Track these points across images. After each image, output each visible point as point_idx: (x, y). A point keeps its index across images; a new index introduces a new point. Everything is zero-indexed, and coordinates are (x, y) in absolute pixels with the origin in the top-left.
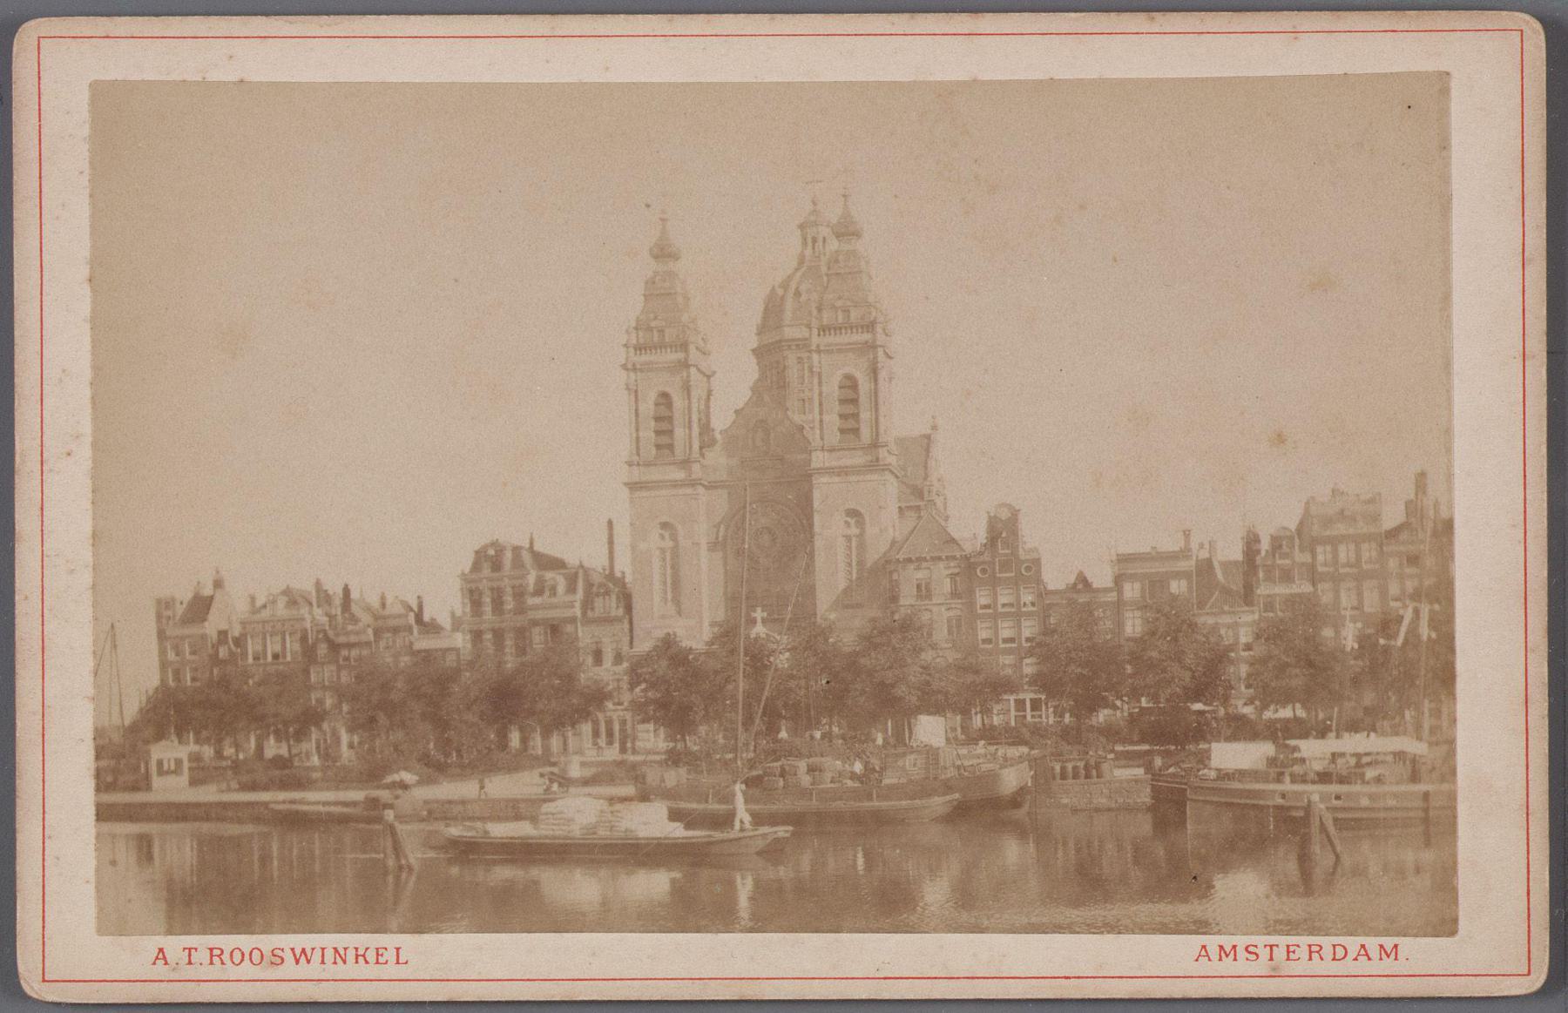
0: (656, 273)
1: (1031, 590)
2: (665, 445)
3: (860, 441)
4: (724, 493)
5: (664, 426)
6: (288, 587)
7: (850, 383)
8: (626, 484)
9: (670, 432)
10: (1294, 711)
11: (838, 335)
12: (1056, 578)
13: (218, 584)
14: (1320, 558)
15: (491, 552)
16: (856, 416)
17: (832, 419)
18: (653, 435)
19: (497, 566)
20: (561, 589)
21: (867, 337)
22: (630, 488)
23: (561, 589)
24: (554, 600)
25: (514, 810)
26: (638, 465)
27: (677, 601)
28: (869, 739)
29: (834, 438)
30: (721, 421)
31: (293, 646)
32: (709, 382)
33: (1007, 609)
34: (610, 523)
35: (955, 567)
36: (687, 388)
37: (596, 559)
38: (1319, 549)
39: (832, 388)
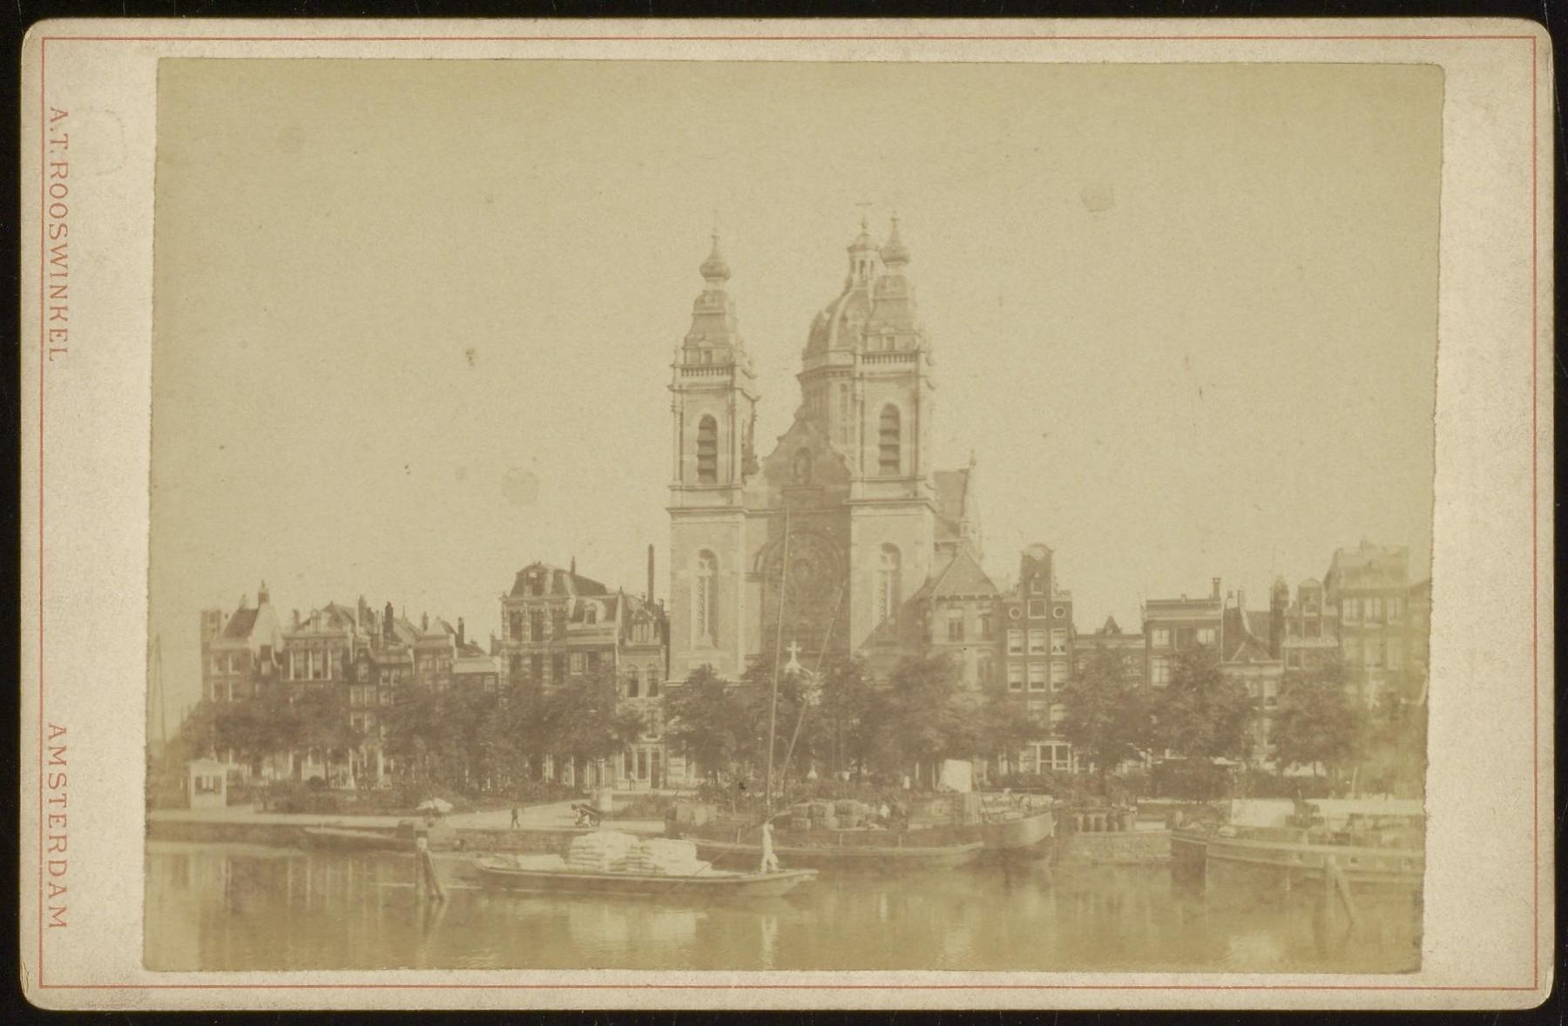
0: (705, 293)
1: (1062, 634)
2: (708, 472)
3: (898, 472)
4: (764, 521)
5: (708, 451)
6: (332, 603)
7: (891, 413)
8: (668, 509)
9: (714, 457)
10: (1315, 769)
11: (887, 363)
12: (1087, 622)
13: (263, 598)
14: (1346, 611)
15: (533, 575)
16: (896, 448)
17: (873, 449)
18: (697, 460)
19: (538, 589)
20: (601, 613)
21: (909, 366)
22: (672, 513)
23: (601, 613)
24: (592, 626)
25: (559, 842)
26: (681, 490)
27: (713, 632)
28: (897, 782)
29: (873, 468)
30: (764, 447)
31: (334, 663)
32: (753, 406)
33: (1038, 653)
34: (651, 549)
35: (987, 607)
36: (731, 411)
37: (637, 588)
38: (1346, 603)
39: (874, 419)
